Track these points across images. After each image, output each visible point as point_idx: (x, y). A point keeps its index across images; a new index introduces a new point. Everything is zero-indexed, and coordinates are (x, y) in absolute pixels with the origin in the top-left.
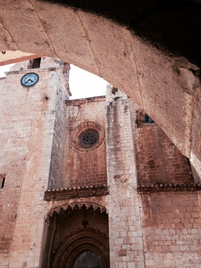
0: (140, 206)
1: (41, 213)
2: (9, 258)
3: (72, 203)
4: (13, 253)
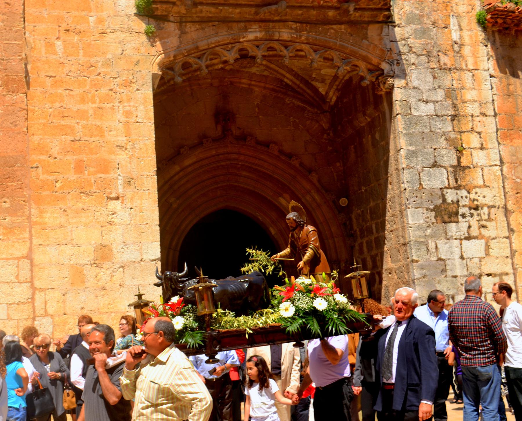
0: (492, 71)
1: (137, 63)
2: (30, 232)
3: (256, 39)
4: (41, 212)
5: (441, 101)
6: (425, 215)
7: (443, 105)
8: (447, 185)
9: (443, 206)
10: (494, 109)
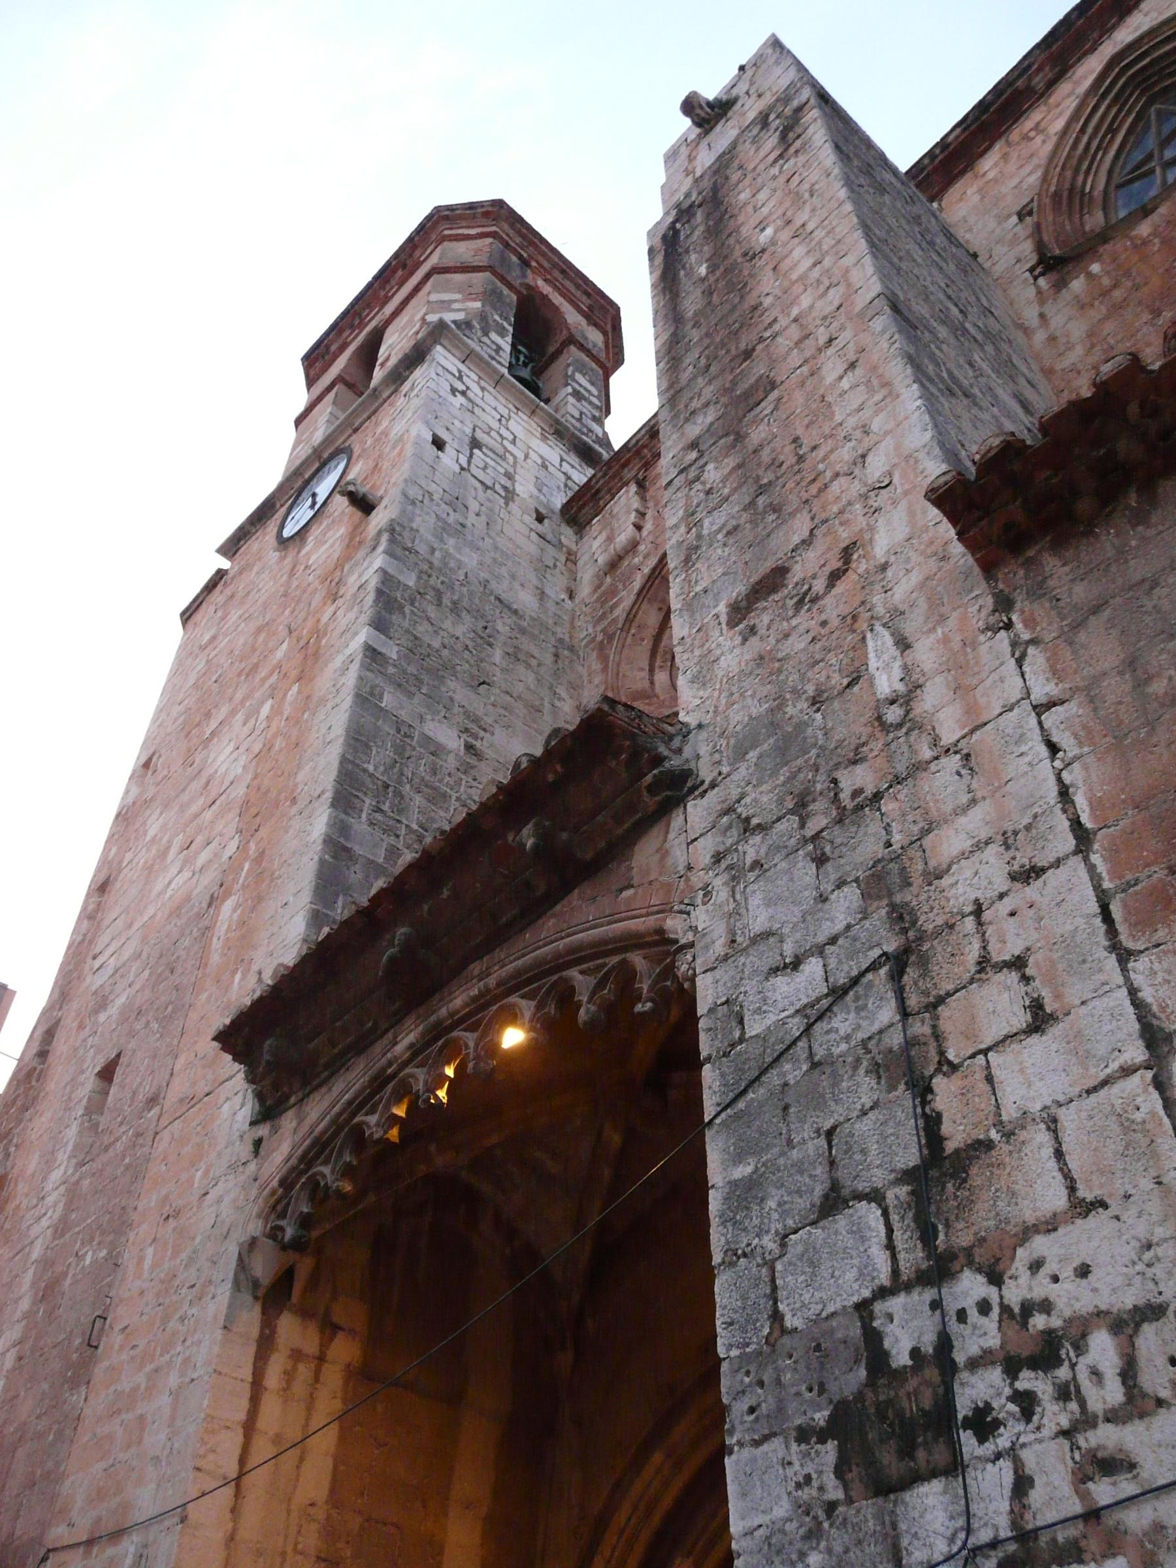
0: (1042, 689)
5: (849, 927)
6: (798, 1470)
7: (855, 939)
8: (884, 1277)
9: (870, 1395)
10: (1076, 824)
